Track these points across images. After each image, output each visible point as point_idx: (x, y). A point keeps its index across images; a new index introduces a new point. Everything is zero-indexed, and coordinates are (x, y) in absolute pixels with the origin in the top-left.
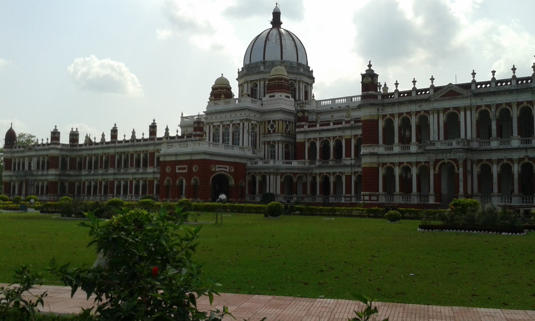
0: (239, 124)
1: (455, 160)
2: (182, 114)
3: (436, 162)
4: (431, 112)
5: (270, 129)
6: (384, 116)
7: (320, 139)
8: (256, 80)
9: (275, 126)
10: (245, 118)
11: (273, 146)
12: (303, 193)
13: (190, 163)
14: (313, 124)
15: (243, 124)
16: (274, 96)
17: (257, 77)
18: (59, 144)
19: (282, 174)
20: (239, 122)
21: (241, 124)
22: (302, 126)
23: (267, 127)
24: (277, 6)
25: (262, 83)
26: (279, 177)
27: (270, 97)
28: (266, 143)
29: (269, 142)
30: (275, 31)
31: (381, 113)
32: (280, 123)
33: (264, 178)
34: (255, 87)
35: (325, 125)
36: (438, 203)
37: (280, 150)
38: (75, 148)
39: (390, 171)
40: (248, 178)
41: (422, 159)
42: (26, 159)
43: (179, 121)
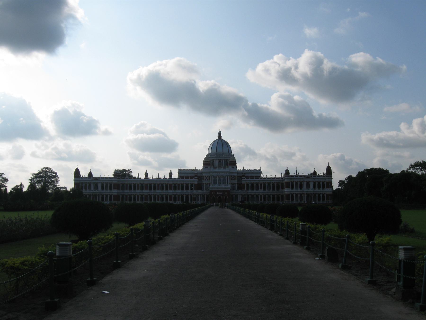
1: (311, 193)
2: (179, 168)
3: (307, 193)
5: (232, 179)
6: (291, 181)
7: (251, 183)
9: (234, 178)
13: (223, 191)
14: (248, 177)
15: (227, 177)
21: (227, 177)
22: (244, 179)
24: (220, 131)
25: (223, 161)
27: (232, 167)
33: (236, 196)
37: (236, 186)
41: (301, 193)
43: (178, 171)
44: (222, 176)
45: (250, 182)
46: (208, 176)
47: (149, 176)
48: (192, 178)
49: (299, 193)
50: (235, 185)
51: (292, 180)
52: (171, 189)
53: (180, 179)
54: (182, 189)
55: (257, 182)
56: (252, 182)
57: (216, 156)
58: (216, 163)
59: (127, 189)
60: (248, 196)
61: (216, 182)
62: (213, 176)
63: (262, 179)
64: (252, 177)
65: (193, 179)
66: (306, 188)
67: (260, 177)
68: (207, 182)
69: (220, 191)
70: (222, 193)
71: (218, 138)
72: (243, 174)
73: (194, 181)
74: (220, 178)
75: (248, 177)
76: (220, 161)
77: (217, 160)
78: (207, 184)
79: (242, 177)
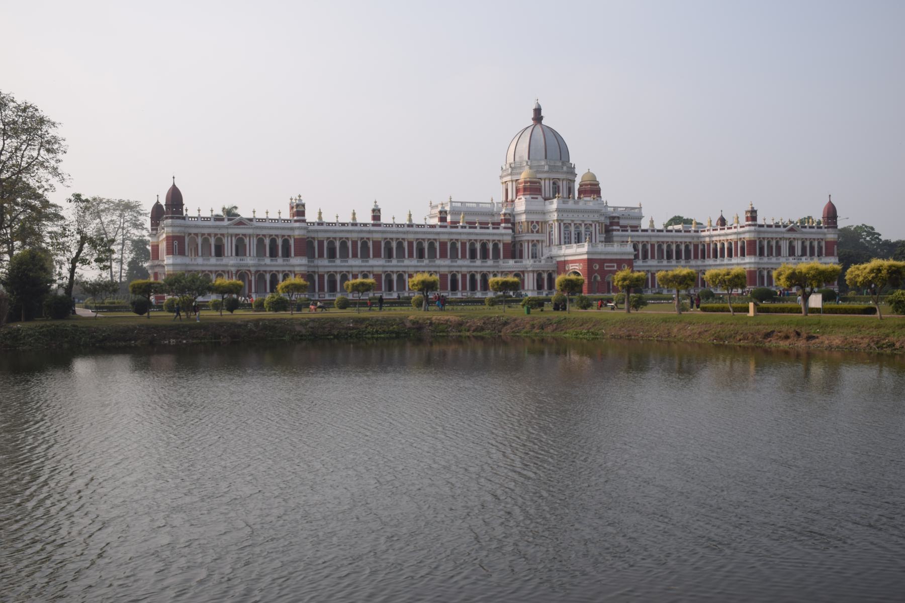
0: (591, 225)
8: (559, 179)
10: (597, 220)
18: (304, 221)
20: (591, 223)
22: (618, 230)
30: (538, 129)
44: (583, 221)
46: (537, 222)
47: (385, 219)
48: (496, 225)
53: (468, 227)
54: (473, 256)
55: (645, 239)
57: (546, 168)
58: (547, 186)
59: (321, 255)
61: (570, 238)
62: (562, 221)
63: (656, 233)
65: (498, 228)
68: (535, 237)
69: (611, 261)
71: (532, 122)
72: (616, 220)
73: (502, 235)
74: (577, 226)
77: (549, 179)
78: (535, 244)
79: (615, 228)
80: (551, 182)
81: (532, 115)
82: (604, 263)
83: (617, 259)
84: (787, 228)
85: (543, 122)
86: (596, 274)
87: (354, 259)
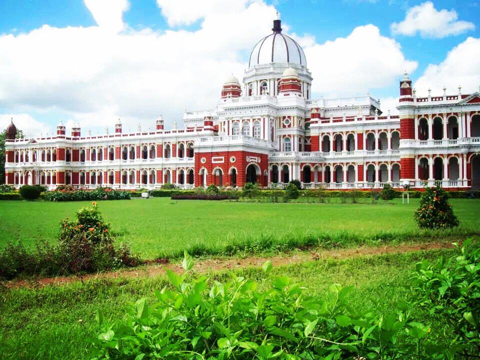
0: (260, 119)
3: (469, 154)
4: (459, 115)
5: (285, 124)
6: (419, 116)
9: (290, 122)
10: (267, 114)
11: (288, 139)
12: (319, 181)
13: (228, 154)
15: (264, 119)
16: (289, 95)
17: (268, 77)
19: (302, 164)
22: (317, 122)
23: (282, 122)
25: (272, 82)
26: (299, 167)
27: (285, 95)
28: (282, 137)
29: (284, 136)
31: (417, 113)
32: (295, 118)
33: (286, 167)
34: (264, 86)
35: (338, 121)
36: (470, 187)
37: (294, 143)
38: (77, 141)
39: (424, 161)
40: (270, 168)
41: (453, 152)
42: (29, 151)
45: (331, 131)
49: (445, 152)
50: (292, 139)
51: (423, 112)
52: (160, 155)
56: (338, 131)
60: (328, 168)
64: (350, 119)
65: (200, 130)
66: (469, 135)
67: (359, 117)
69: (218, 154)
70: (213, 160)
71: (272, 32)
74: (246, 122)
75: (325, 120)
76: (265, 84)
77: (257, 81)
79: (312, 120)
80: (259, 85)
81: (272, 25)
82: (212, 156)
83: (225, 152)
84: (468, 98)
85: (282, 32)
86: (203, 168)
87: (159, 158)
